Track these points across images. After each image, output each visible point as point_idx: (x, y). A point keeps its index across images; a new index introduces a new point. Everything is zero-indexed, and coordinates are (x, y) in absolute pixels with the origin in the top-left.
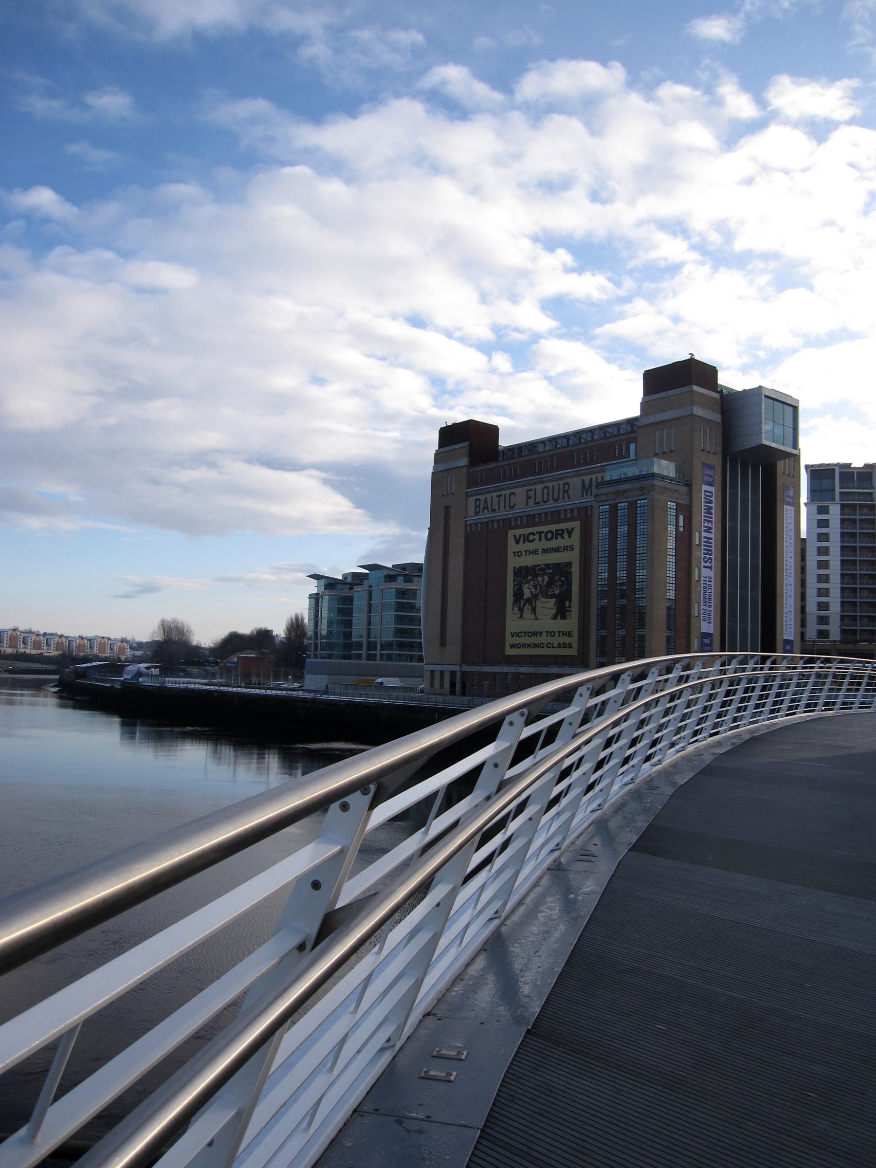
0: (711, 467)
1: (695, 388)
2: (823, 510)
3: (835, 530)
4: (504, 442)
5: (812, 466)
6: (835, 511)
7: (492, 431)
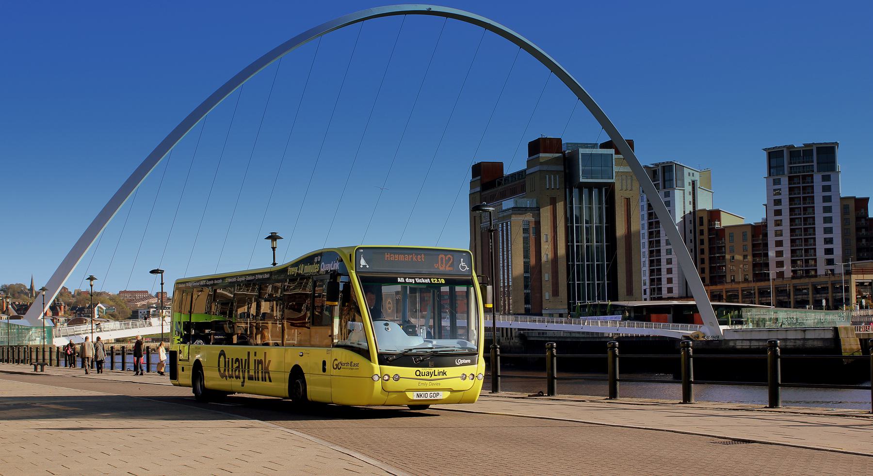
1: (541, 155)
2: (777, 182)
3: (785, 197)
4: (507, 171)
6: (785, 181)
7: (499, 166)
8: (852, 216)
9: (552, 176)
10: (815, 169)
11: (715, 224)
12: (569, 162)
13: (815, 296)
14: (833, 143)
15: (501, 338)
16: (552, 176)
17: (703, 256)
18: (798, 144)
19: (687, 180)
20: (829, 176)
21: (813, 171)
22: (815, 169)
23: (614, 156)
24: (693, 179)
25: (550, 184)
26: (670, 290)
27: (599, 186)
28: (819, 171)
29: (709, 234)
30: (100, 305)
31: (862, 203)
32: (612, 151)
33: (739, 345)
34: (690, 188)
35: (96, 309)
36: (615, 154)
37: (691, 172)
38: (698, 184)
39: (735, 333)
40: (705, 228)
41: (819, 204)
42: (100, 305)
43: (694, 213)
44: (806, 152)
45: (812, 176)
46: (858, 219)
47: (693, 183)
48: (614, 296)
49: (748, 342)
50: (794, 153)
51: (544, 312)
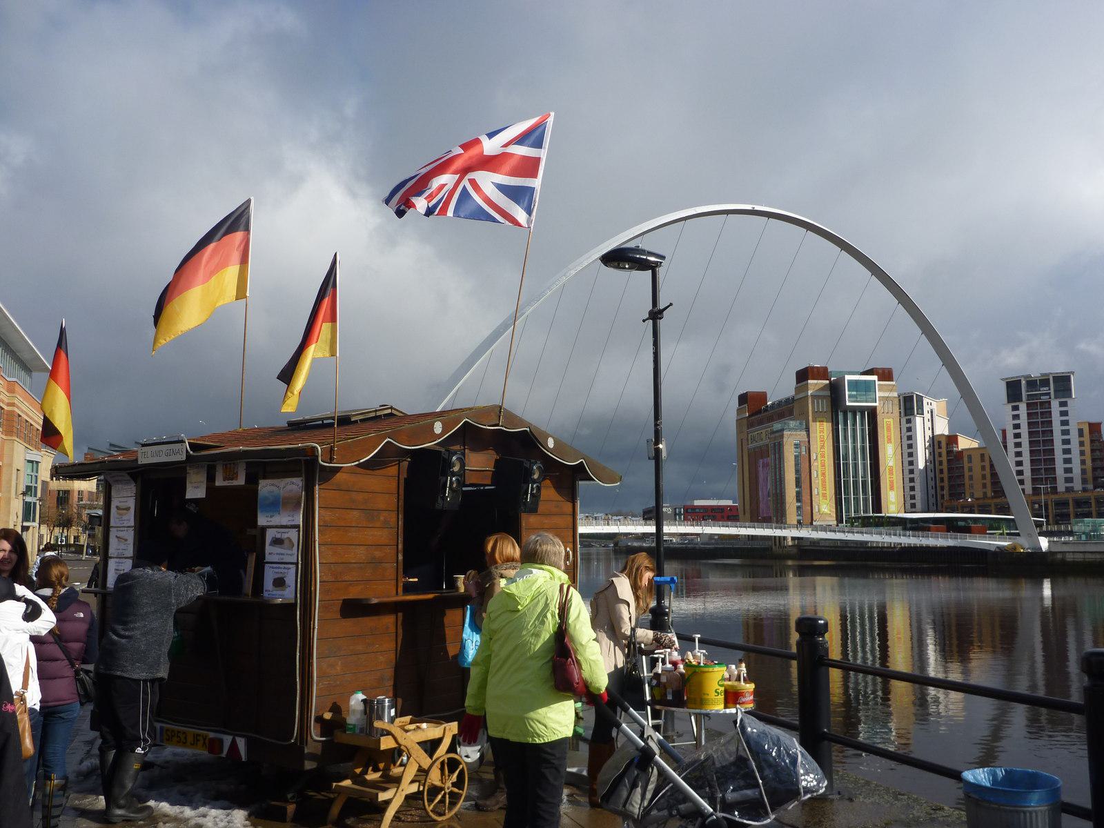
1: (809, 381)
2: (1016, 408)
3: (1024, 421)
5: (1007, 379)
6: (1023, 407)
8: (1087, 439)
10: (1052, 396)
12: (835, 391)
13: (1076, 510)
14: (1069, 373)
15: (774, 547)
16: (820, 401)
18: (1035, 374)
19: (926, 408)
20: (1066, 402)
21: (1050, 398)
22: (1052, 396)
23: (877, 383)
27: (862, 410)
28: (1056, 398)
29: (948, 456)
31: (1094, 428)
32: (875, 378)
33: (1069, 558)
34: (929, 415)
36: (879, 380)
37: (930, 401)
38: (935, 413)
39: (1064, 545)
40: (944, 451)
41: (1057, 428)
43: (933, 438)
44: (1045, 382)
45: (1049, 403)
46: (1092, 441)
48: (878, 506)
49: (1081, 554)
50: (1032, 384)
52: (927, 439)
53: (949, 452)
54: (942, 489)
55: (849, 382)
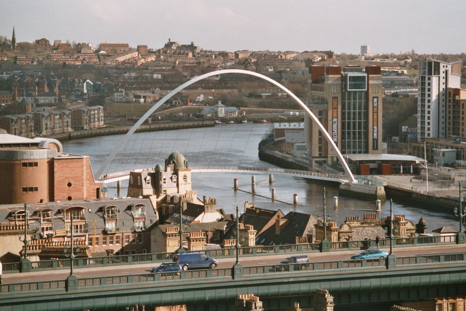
0: (337, 98)
9: (335, 87)
11: (456, 98)
16: (335, 87)
17: (449, 115)
19: (442, 70)
24: (446, 69)
25: (334, 91)
26: (429, 135)
29: (453, 103)
30: (88, 81)
34: (444, 75)
35: (85, 84)
38: (450, 72)
40: (451, 98)
42: (88, 81)
43: (447, 88)
47: (446, 71)
51: (328, 156)
52: (441, 90)
53: (454, 100)
54: (449, 124)
55: (350, 77)
